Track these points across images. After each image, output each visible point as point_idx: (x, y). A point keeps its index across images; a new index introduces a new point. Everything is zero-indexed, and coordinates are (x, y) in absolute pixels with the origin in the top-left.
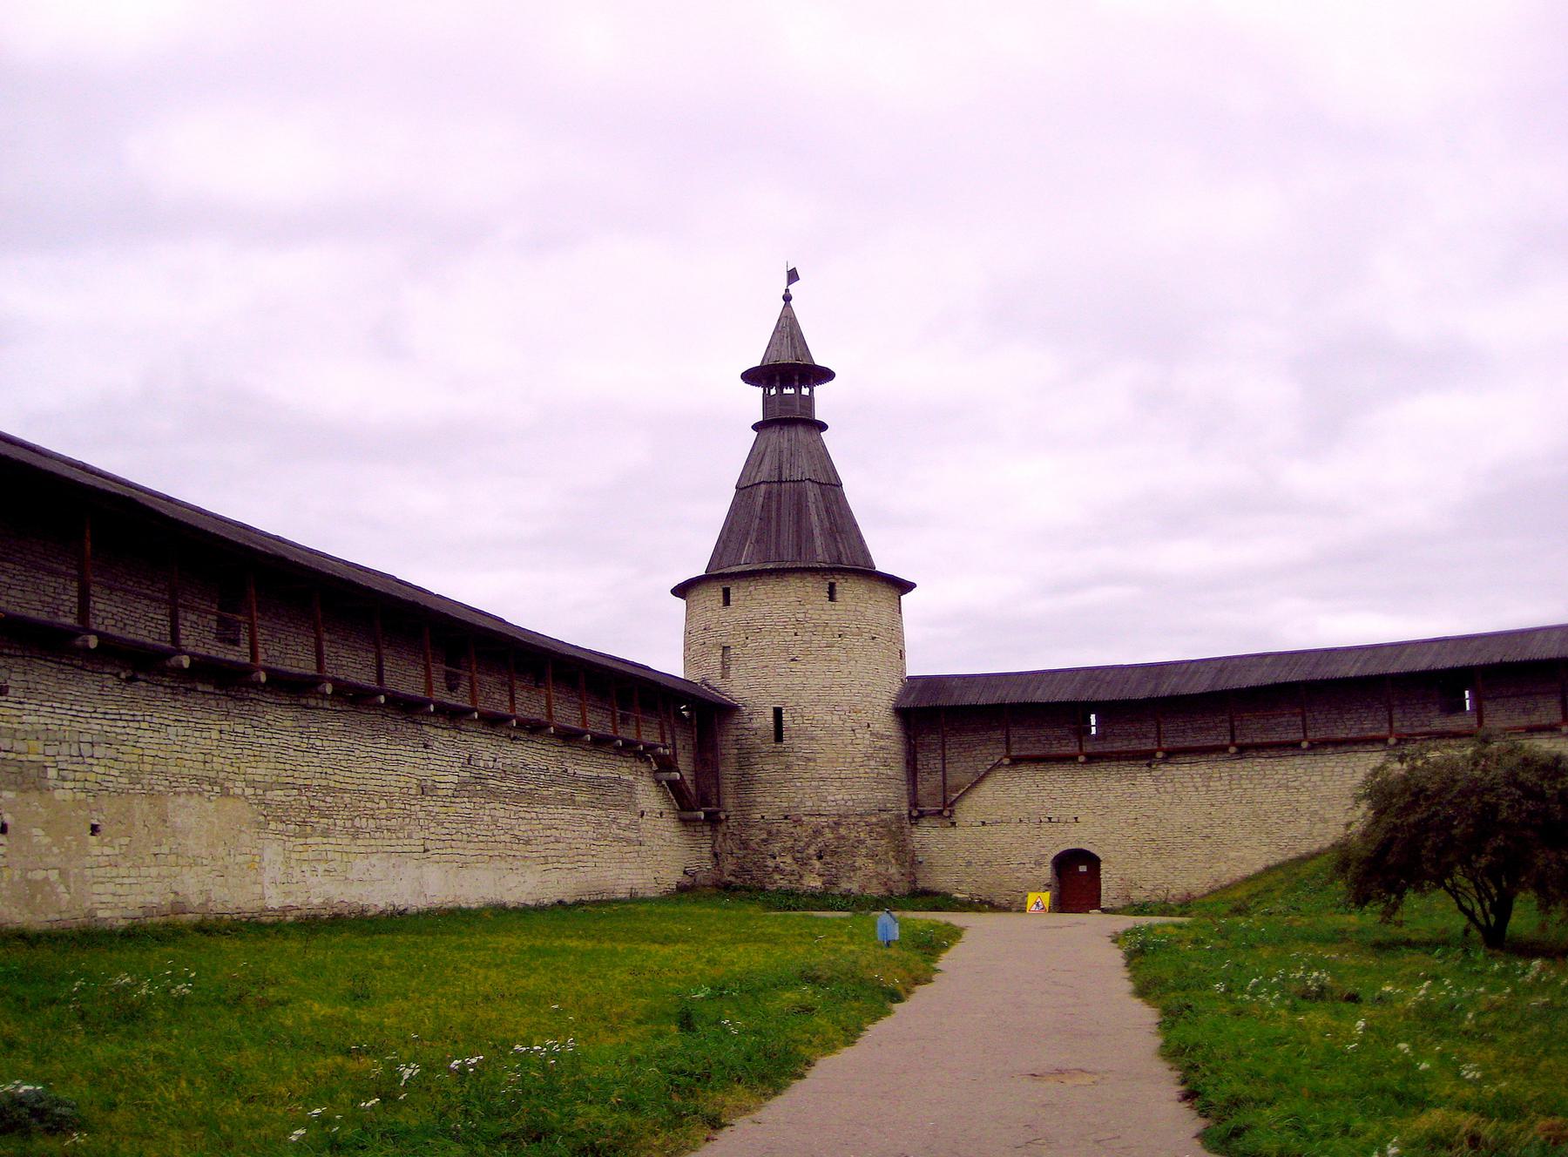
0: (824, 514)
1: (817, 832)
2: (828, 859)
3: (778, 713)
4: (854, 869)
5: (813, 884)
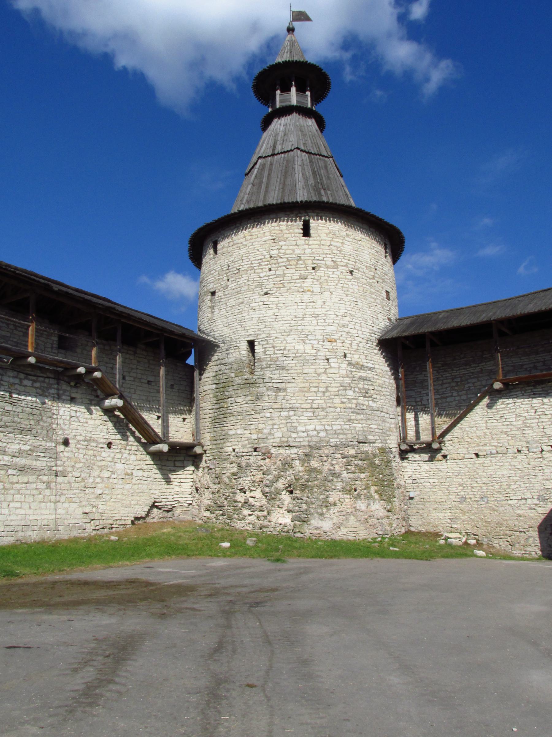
0: (309, 173)
1: (287, 464)
2: (297, 493)
3: (251, 344)
4: (327, 504)
5: (282, 521)
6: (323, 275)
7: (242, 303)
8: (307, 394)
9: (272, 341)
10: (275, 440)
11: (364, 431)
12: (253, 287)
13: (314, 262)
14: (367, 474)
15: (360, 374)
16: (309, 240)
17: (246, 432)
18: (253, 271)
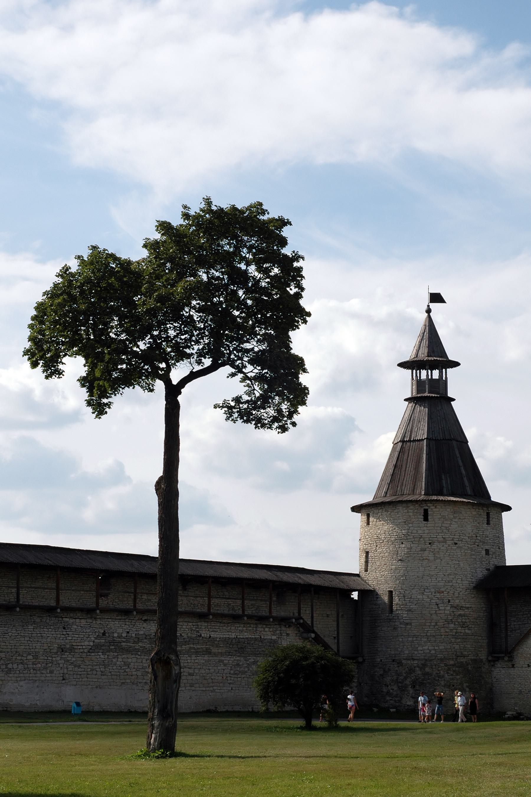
1: (411, 670)
2: (417, 687)
5: (409, 703)
6: (436, 548)
8: (424, 627)
10: (405, 655)
11: (460, 649)
14: (461, 676)
15: (459, 613)
16: (427, 524)
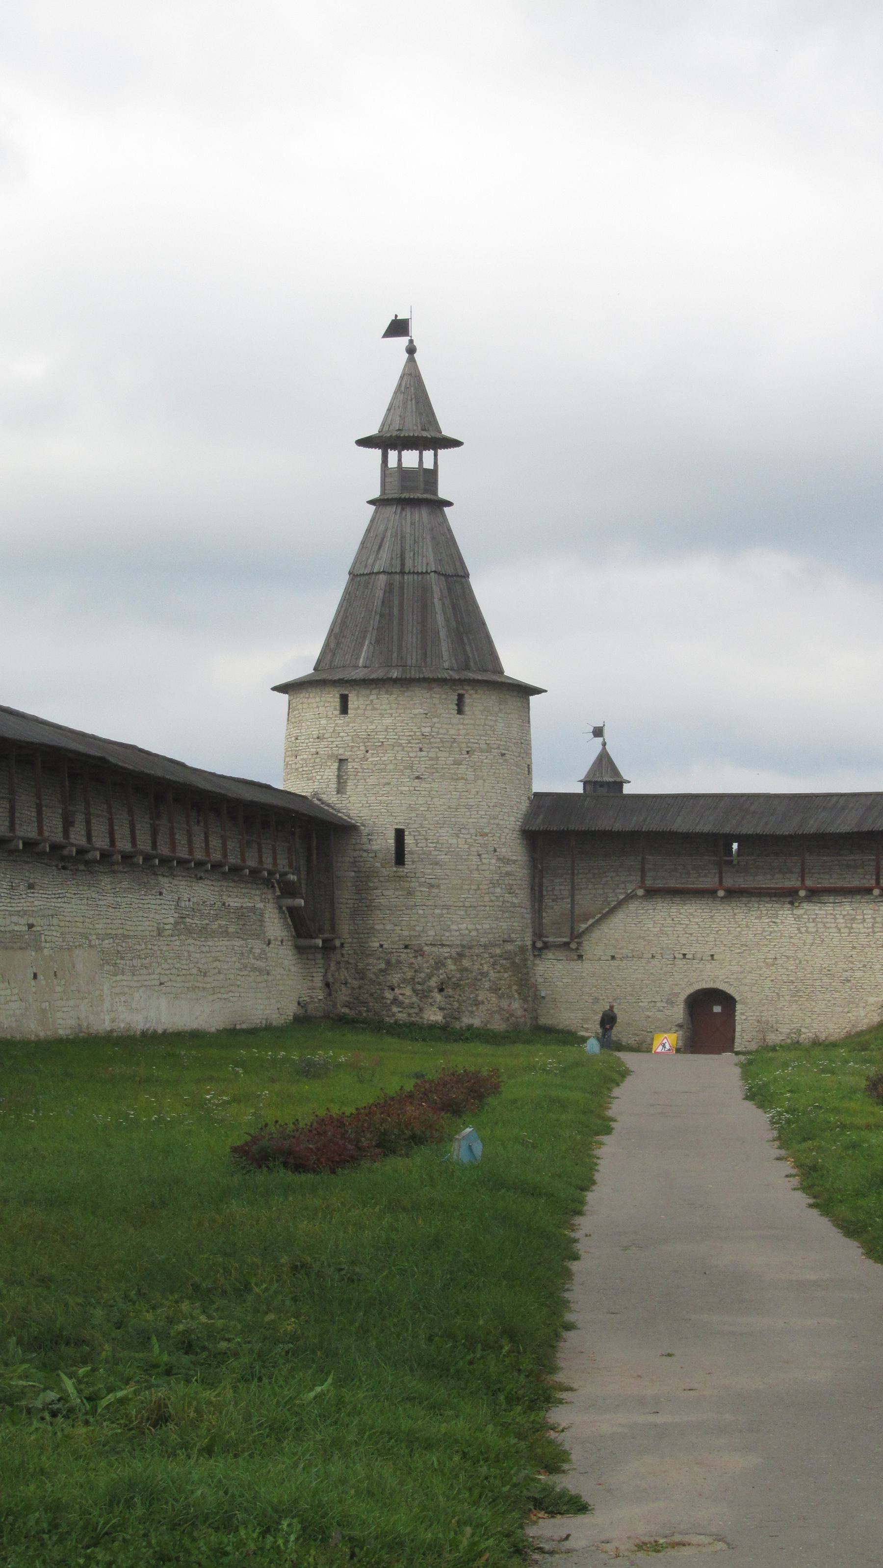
1: (440, 963)
3: (400, 835)
4: (477, 1003)
5: (433, 1018)
7: (389, 784)
9: (424, 833)
12: (402, 768)
13: (469, 745)
14: (510, 973)
17: (396, 928)
18: (400, 748)
